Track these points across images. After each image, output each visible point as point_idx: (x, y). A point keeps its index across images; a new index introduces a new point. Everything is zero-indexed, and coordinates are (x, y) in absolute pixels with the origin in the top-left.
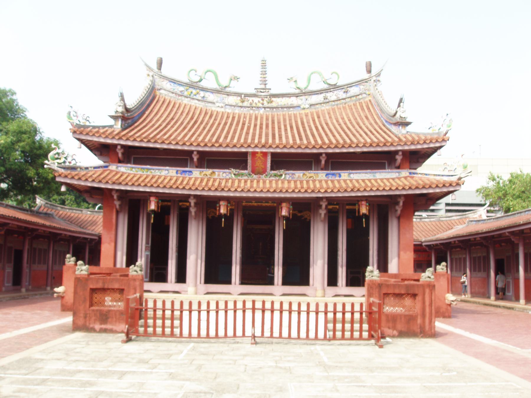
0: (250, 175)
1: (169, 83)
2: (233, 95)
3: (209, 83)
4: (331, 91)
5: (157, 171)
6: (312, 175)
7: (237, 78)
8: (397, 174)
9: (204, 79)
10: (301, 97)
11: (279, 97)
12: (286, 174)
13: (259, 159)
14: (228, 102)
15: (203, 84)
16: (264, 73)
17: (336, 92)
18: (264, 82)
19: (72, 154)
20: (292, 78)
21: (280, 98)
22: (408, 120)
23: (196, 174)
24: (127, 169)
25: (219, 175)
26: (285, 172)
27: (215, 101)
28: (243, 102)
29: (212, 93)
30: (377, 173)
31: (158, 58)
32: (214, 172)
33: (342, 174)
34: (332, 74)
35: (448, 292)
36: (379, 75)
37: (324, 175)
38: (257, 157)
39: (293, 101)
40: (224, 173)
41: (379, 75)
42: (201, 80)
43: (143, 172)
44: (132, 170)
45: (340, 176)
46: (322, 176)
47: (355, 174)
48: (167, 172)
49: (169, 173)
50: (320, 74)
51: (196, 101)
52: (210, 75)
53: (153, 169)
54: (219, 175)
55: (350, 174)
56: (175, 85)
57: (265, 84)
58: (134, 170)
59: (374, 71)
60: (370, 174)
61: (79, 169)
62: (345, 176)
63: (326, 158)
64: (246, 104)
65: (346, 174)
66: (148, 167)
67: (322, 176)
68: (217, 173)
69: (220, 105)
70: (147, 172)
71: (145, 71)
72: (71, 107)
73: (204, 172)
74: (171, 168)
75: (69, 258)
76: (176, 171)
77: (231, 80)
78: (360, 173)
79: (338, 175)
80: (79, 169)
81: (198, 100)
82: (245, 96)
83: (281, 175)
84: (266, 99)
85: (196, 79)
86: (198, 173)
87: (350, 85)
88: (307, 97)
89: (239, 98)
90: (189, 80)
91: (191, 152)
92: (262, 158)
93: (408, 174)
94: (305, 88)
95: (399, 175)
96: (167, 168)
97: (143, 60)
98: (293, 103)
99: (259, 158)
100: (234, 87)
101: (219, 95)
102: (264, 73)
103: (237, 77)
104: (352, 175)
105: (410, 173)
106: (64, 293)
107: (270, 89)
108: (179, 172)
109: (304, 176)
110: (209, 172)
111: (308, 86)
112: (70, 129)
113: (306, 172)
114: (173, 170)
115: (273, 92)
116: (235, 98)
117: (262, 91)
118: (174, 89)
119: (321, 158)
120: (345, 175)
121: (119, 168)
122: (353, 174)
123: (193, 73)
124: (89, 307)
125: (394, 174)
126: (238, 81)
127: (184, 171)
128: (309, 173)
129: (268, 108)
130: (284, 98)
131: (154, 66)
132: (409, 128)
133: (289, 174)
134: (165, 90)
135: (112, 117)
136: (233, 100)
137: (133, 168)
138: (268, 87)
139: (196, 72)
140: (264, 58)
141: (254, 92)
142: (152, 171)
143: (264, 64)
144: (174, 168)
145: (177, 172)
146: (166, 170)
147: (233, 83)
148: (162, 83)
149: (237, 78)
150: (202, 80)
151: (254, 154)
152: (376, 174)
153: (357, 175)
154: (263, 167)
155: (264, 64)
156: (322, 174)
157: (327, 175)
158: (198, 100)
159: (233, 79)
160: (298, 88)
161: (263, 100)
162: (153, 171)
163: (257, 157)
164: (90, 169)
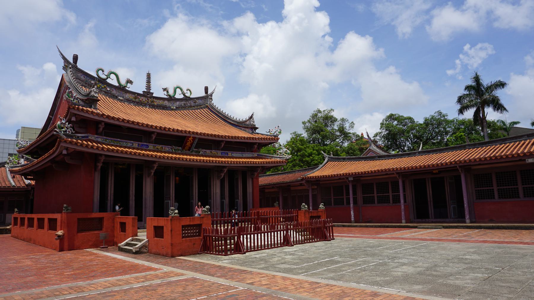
1: (83, 76)
2: (129, 93)
3: (112, 81)
4: (187, 101)
5: (124, 143)
6: (215, 153)
9: (110, 78)
10: (171, 102)
11: (158, 100)
14: (126, 98)
15: (109, 81)
16: (149, 82)
17: (189, 102)
18: (149, 87)
21: (159, 100)
22: (256, 126)
23: (151, 147)
24: (103, 139)
25: (165, 149)
27: (116, 95)
28: (135, 98)
29: (115, 89)
30: (244, 153)
33: (229, 153)
34: (187, 90)
38: (189, 139)
39: (166, 103)
41: (211, 95)
44: (106, 141)
45: (228, 154)
48: (131, 144)
49: (133, 145)
50: (181, 89)
51: (104, 93)
52: (113, 76)
53: (122, 142)
54: (165, 149)
55: (232, 153)
56: (88, 78)
57: (151, 89)
58: (108, 141)
59: (209, 92)
64: (137, 100)
65: (230, 153)
66: (119, 140)
69: (121, 98)
71: (62, 63)
73: (157, 147)
74: (134, 142)
78: (237, 153)
81: (104, 91)
82: (137, 95)
84: (150, 99)
85: (104, 77)
86: (152, 147)
87: (198, 98)
88: (174, 102)
89: (133, 96)
90: (98, 76)
92: (191, 141)
93: (257, 155)
94: (174, 96)
96: (132, 142)
97: (62, 54)
98: (166, 104)
99: (190, 140)
101: (120, 91)
102: (149, 82)
104: (233, 154)
105: (258, 155)
106: (63, 236)
107: (152, 93)
108: (140, 145)
111: (175, 95)
114: (136, 143)
115: (154, 95)
116: (131, 95)
117: (148, 94)
118: (87, 81)
119: (222, 143)
126: (132, 84)
127: (142, 145)
129: (151, 105)
130: (161, 101)
131: (71, 61)
132: (257, 131)
134: (80, 80)
136: (128, 96)
138: (151, 91)
139: (103, 71)
140: (149, 72)
141: (142, 93)
142: (121, 142)
143: (149, 76)
144: (136, 142)
145: (138, 146)
146: (131, 143)
147: (129, 85)
148: (78, 74)
153: (236, 154)
154: (190, 146)
155: (149, 76)
157: (222, 153)
158: (104, 91)
160: (170, 96)
161: (148, 99)
162: (122, 143)
163: (189, 139)
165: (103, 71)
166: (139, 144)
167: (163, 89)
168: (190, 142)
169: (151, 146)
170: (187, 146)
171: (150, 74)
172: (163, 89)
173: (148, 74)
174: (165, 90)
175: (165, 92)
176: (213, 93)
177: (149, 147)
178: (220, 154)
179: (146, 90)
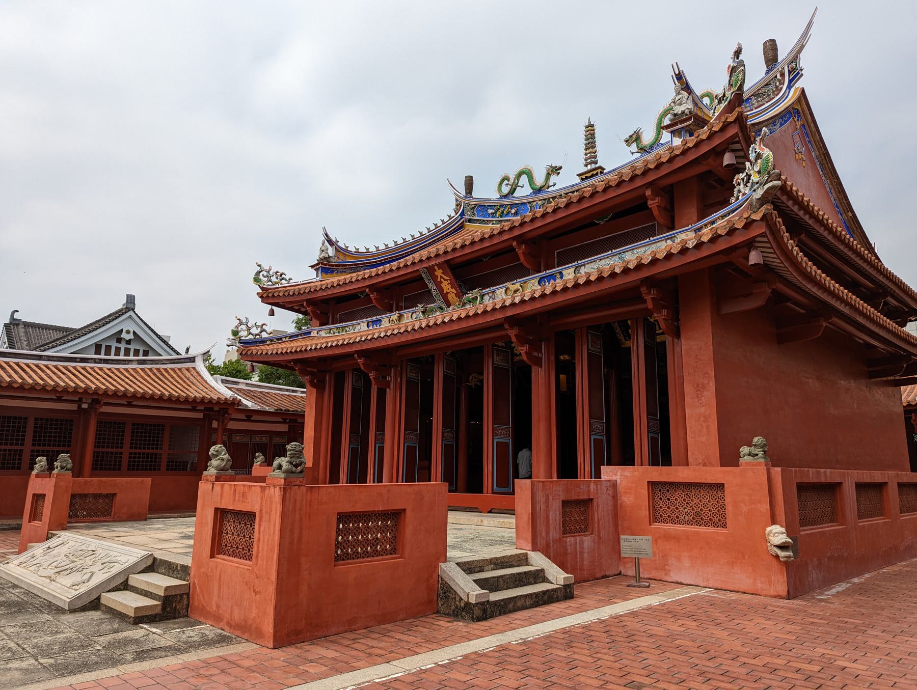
0: (441, 308)
7: (555, 170)
8: (669, 242)
12: (482, 296)
13: (442, 280)
19: (260, 324)
20: (631, 137)
26: (481, 292)
31: (466, 177)
32: (400, 317)
33: (564, 272)
35: (774, 522)
36: (795, 58)
37: (536, 281)
40: (413, 313)
41: (795, 58)
42: (512, 191)
43: (339, 333)
44: (330, 332)
46: (533, 284)
47: (587, 266)
52: (524, 180)
55: (577, 268)
59: (783, 54)
60: (614, 258)
61: (268, 342)
62: (569, 274)
63: (523, 247)
67: (533, 284)
68: (405, 315)
70: (343, 331)
72: (259, 266)
75: (258, 457)
76: (366, 323)
77: (548, 175)
79: (558, 276)
80: (268, 342)
83: (477, 297)
85: (506, 190)
91: (361, 291)
95: (674, 241)
99: (441, 277)
100: (554, 185)
103: (553, 167)
104: (583, 270)
107: (600, 167)
109: (508, 291)
110: (395, 316)
112: (258, 294)
113: (508, 284)
114: (364, 322)
117: (587, 175)
120: (569, 274)
121: (320, 333)
122: (584, 265)
123: (506, 182)
124: (30, 522)
125: (664, 242)
126: (559, 173)
128: (513, 284)
131: (463, 192)
133: (488, 294)
135: (312, 267)
137: (330, 329)
139: (508, 181)
143: (590, 130)
145: (368, 326)
147: (553, 179)
149: (555, 170)
150: (515, 189)
151: (431, 270)
152: (627, 253)
156: (533, 281)
159: (550, 173)
162: (347, 329)
164: (284, 339)
165: (508, 181)
166: (368, 322)
167: (626, 141)
168: (445, 280)
169: (385, 320)
170: (447, 293)
171: (593, 126)
172: (626, 141)
173: (587, 127)
174: (628, 142)
175: (634, 147)
176: (802, 47)
177: (383, 322)
178: (537, 284)
179: (585, 169)
